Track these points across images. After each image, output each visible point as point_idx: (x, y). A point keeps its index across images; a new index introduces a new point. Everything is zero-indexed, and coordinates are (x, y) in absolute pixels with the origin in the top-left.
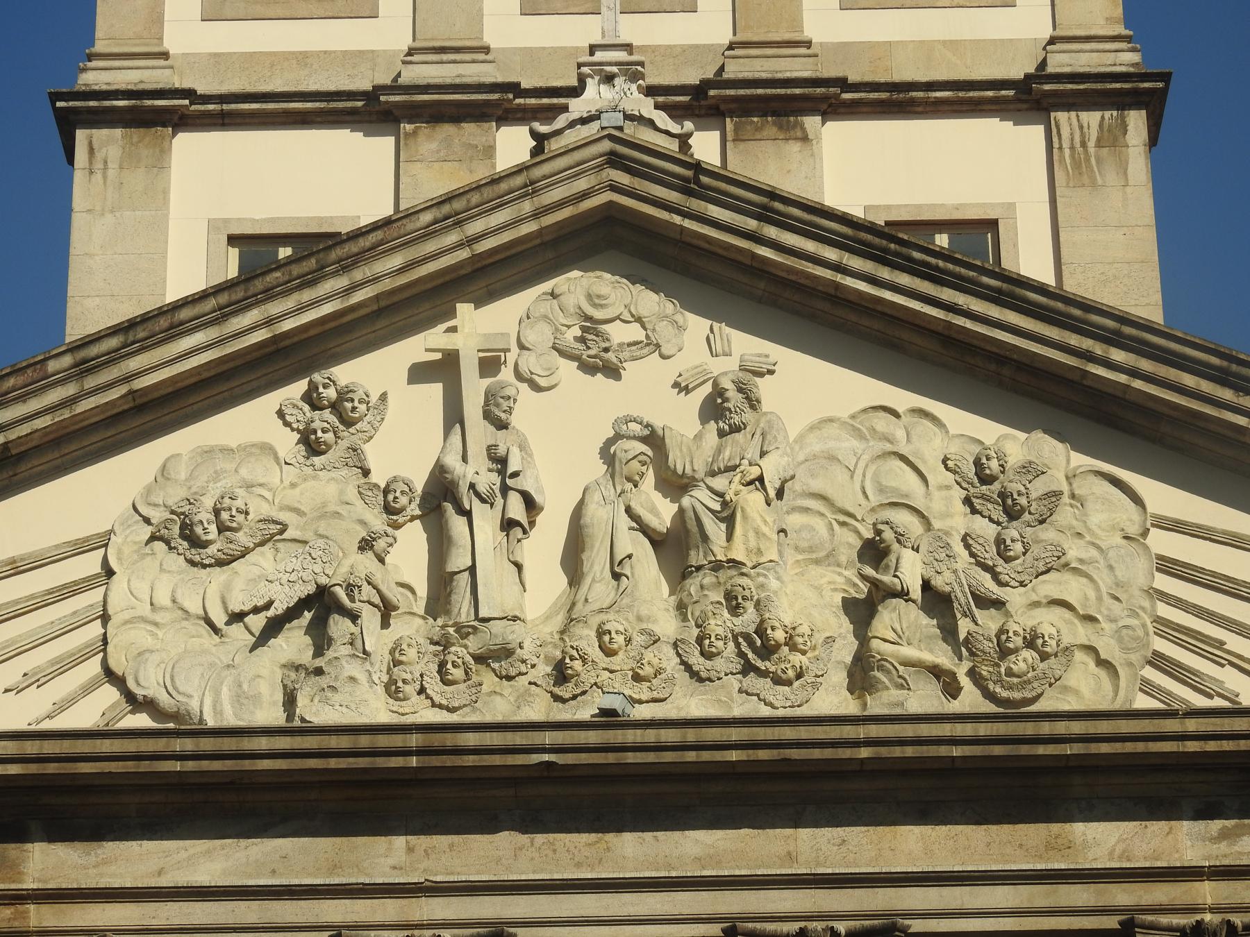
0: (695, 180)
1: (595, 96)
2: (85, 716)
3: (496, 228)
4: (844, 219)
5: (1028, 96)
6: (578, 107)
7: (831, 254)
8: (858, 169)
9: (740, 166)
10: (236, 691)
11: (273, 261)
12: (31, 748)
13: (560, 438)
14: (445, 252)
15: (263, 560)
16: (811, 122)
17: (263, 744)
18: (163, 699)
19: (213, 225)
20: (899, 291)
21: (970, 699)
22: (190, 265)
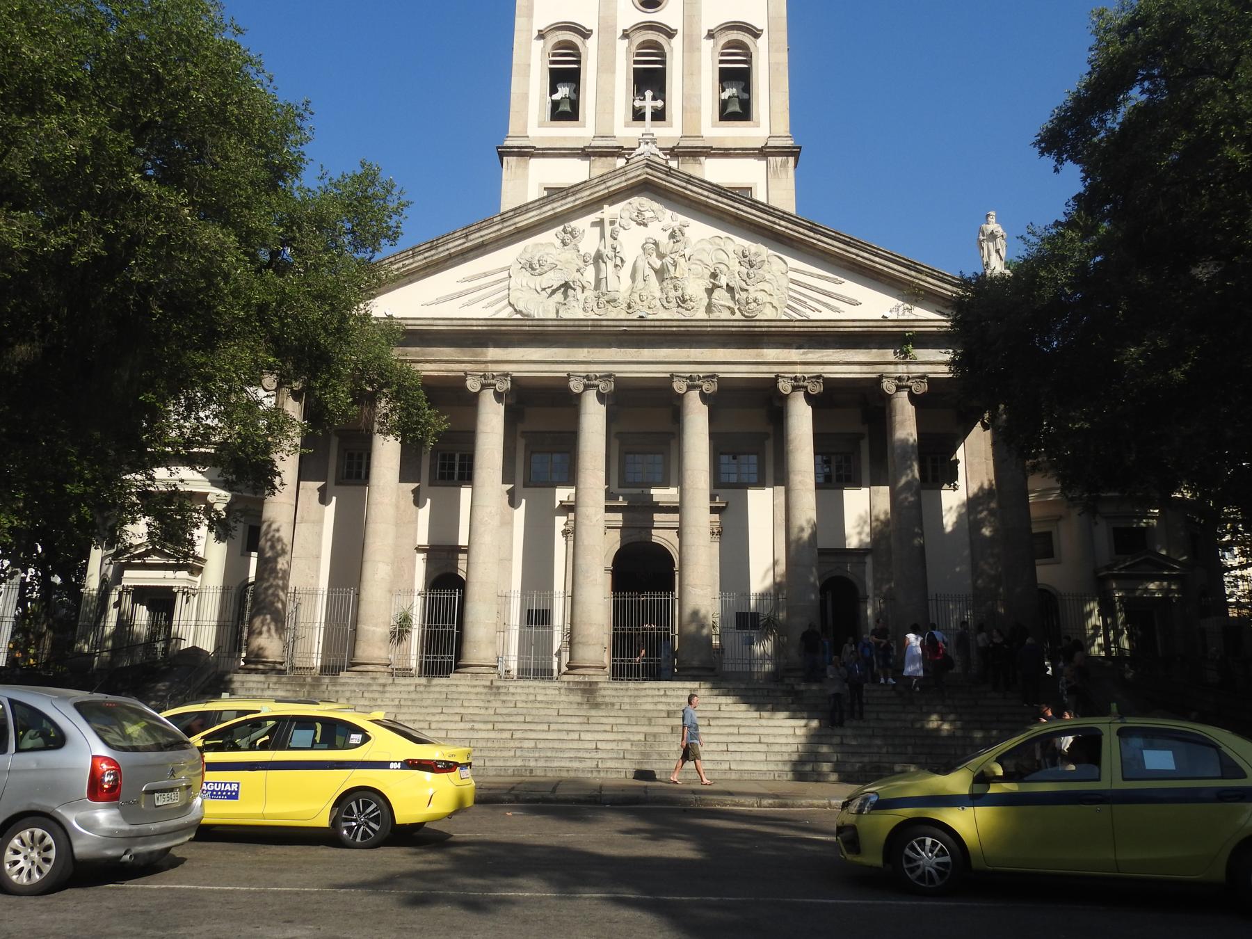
0: (669, 172)
1: (643, 148)
3: (616, 184)
4: (710, 183)
5: (763, 153)
6: (638, 151)
7: (706, 193)
8: (715, 171)
9: (682, 169)
10: (543, 309)
11: (555, 193)
12: (489, 323)
13: (631, 242)
14: (601, 191)
15: (551, 274)
16: (702, 159)
17: (550, 323)
18: (524, 311)
19: (540, 185)
20: (724, 204)
21: (738, 316)
22: (534, 193)
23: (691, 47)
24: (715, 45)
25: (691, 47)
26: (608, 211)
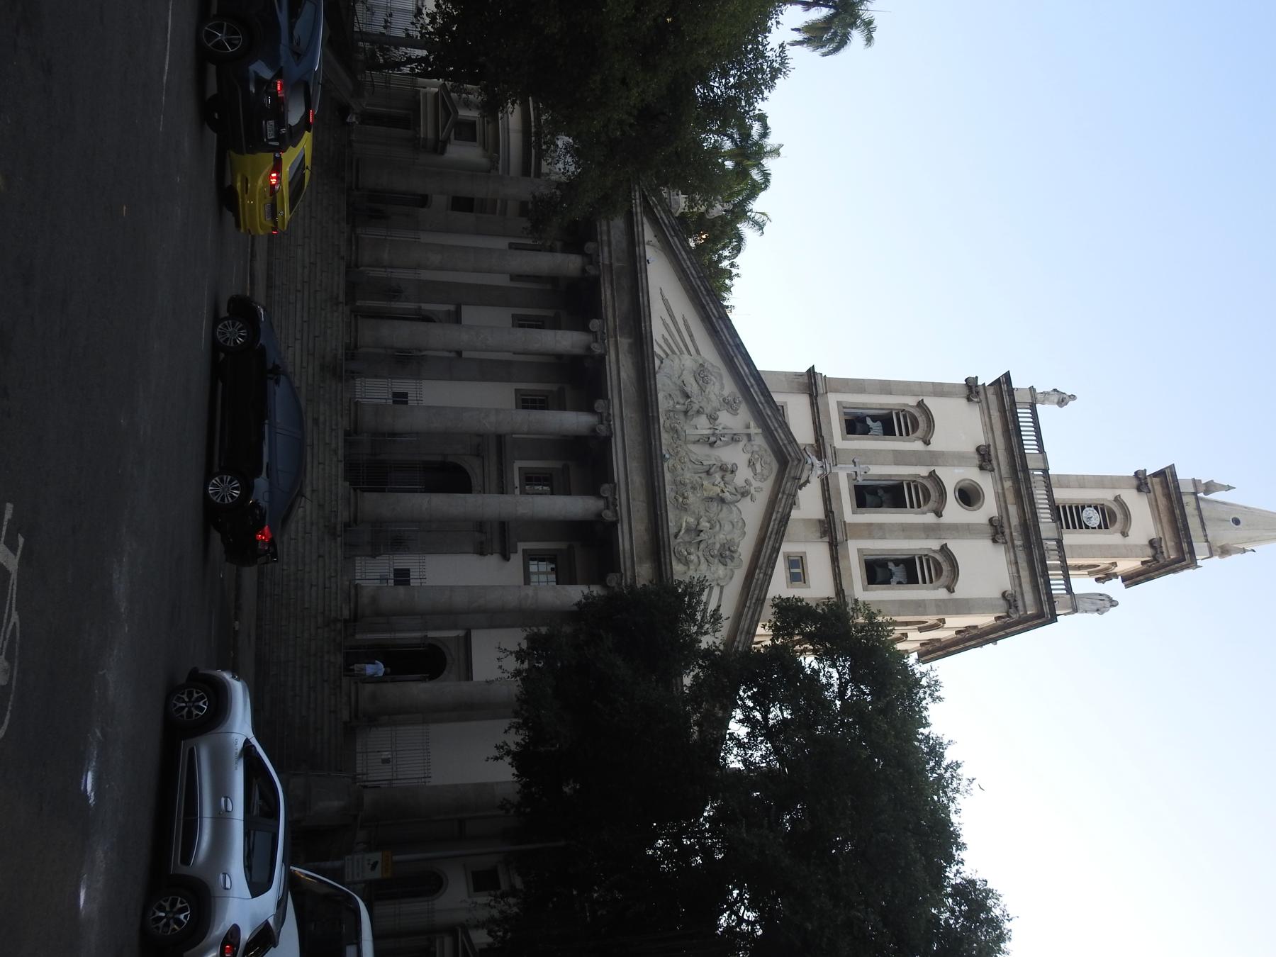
2: (656, 349)
16: (827, 539)
23: (929, 531)
24: (935, 551)
25: (929, 531)
26: (755, 430)
